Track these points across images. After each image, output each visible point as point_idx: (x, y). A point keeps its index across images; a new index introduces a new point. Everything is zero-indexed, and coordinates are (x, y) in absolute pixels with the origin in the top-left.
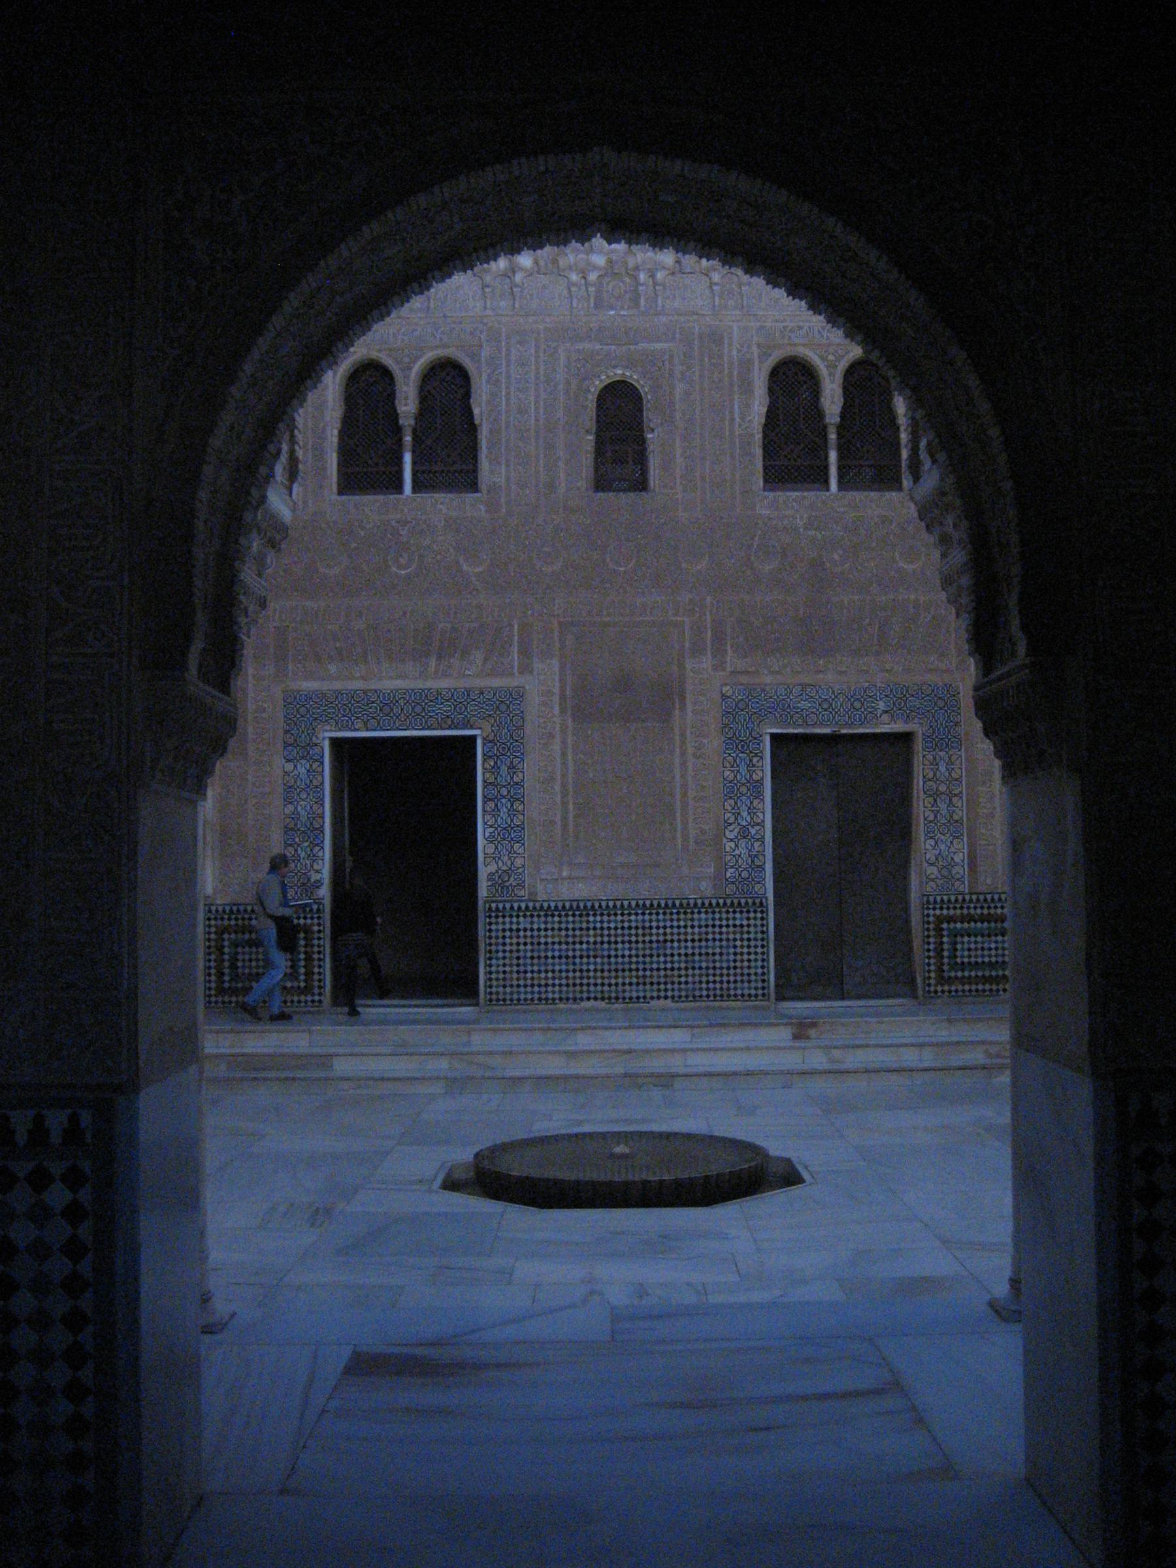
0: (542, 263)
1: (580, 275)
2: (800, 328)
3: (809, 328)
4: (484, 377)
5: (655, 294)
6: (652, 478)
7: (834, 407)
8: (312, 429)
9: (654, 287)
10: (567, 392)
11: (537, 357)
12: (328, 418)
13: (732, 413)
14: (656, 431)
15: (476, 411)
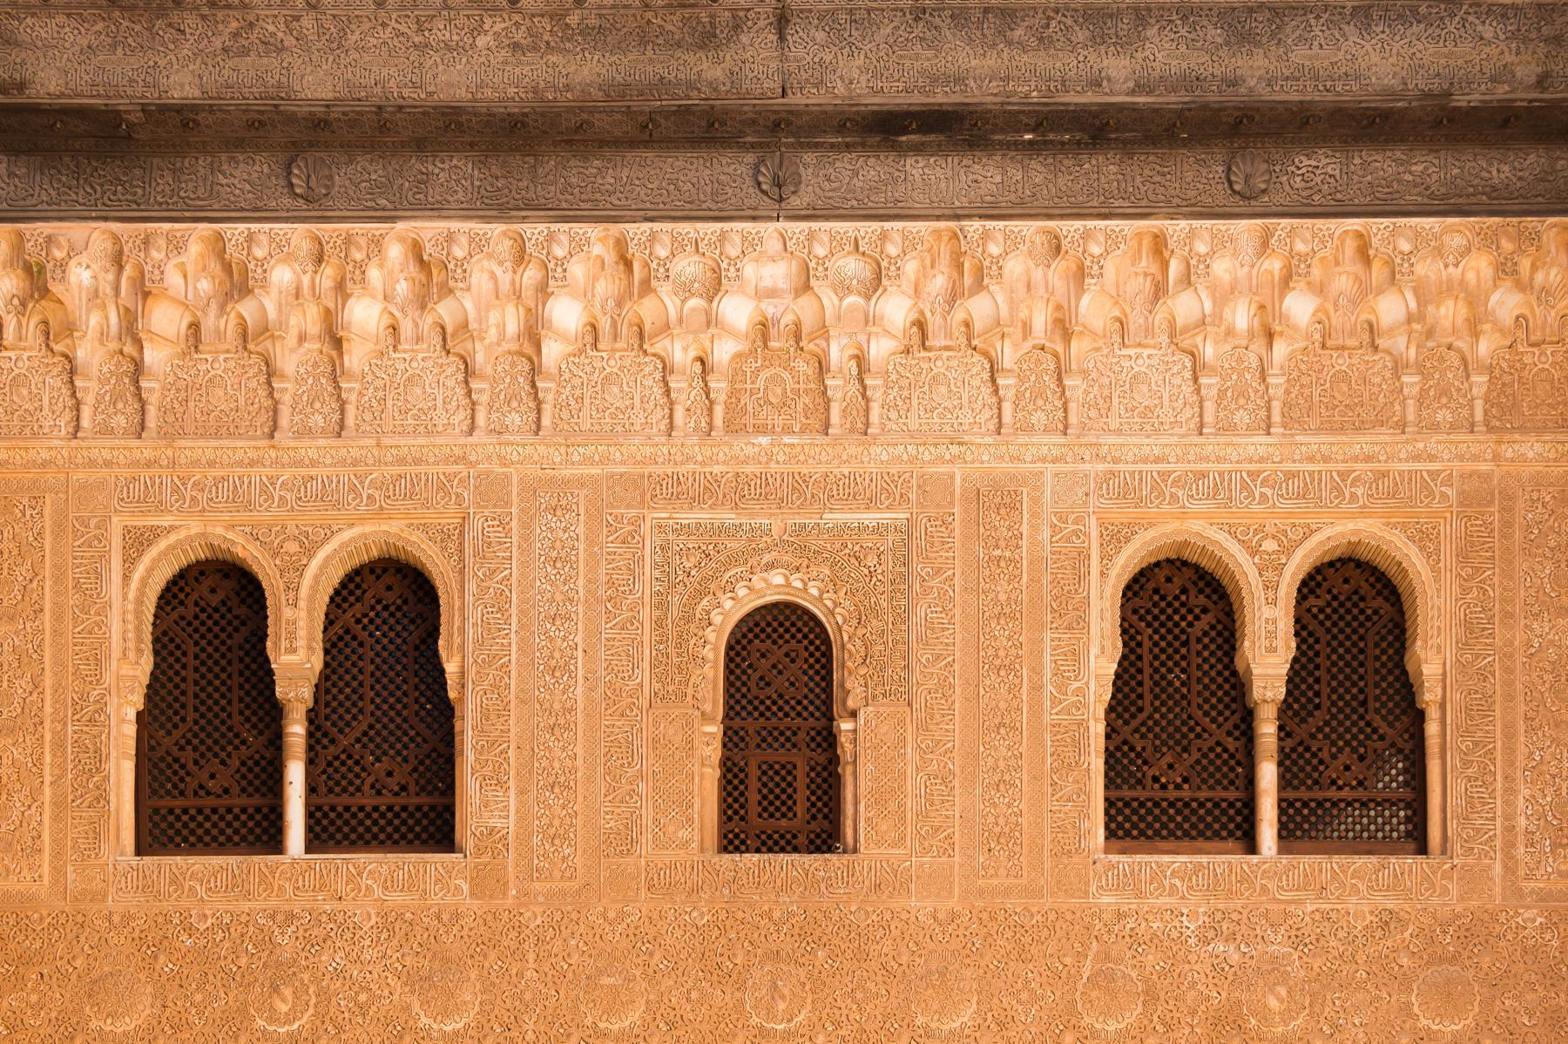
0: (605, 325)
1: (692, 354)
2: (1204, 475)
3: (1221, 474)
4: (472, 586)
5: (864, 395)
6: (849, 823)
7: (1273, 660)
8: (75, 703)
9: (861, 381)
10: (659, 624)
11: (590, 542)
12: (109, 679)
13: (1037, 671)
14: (861, 715)
15: (451, 668)
